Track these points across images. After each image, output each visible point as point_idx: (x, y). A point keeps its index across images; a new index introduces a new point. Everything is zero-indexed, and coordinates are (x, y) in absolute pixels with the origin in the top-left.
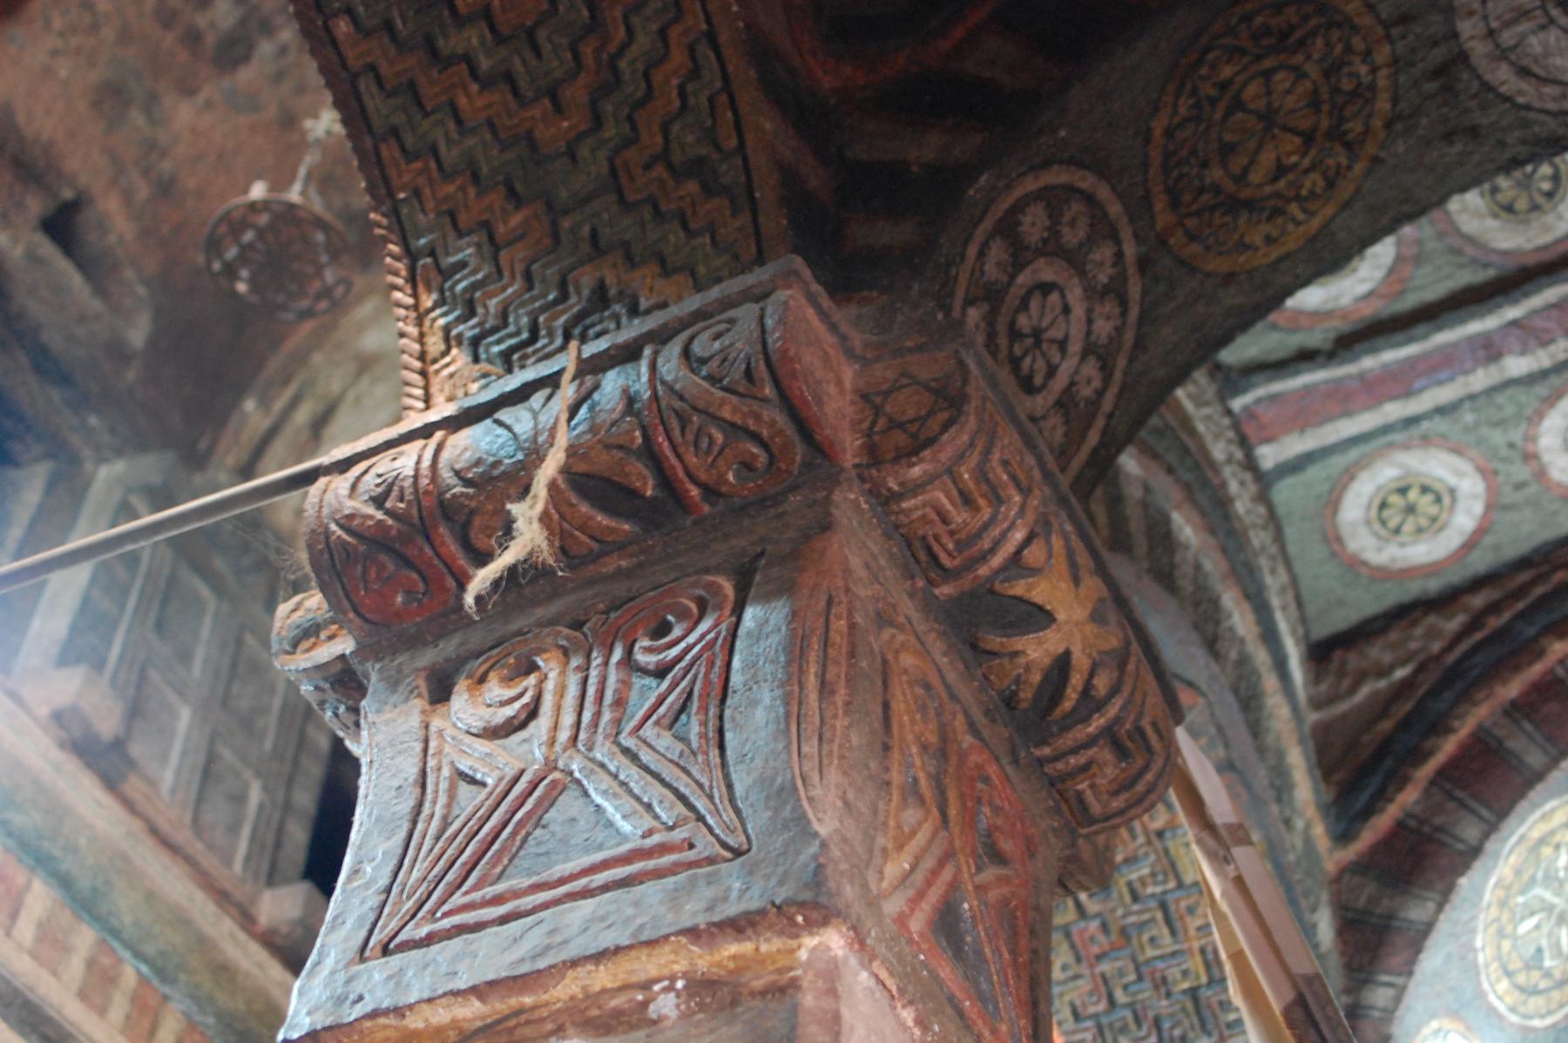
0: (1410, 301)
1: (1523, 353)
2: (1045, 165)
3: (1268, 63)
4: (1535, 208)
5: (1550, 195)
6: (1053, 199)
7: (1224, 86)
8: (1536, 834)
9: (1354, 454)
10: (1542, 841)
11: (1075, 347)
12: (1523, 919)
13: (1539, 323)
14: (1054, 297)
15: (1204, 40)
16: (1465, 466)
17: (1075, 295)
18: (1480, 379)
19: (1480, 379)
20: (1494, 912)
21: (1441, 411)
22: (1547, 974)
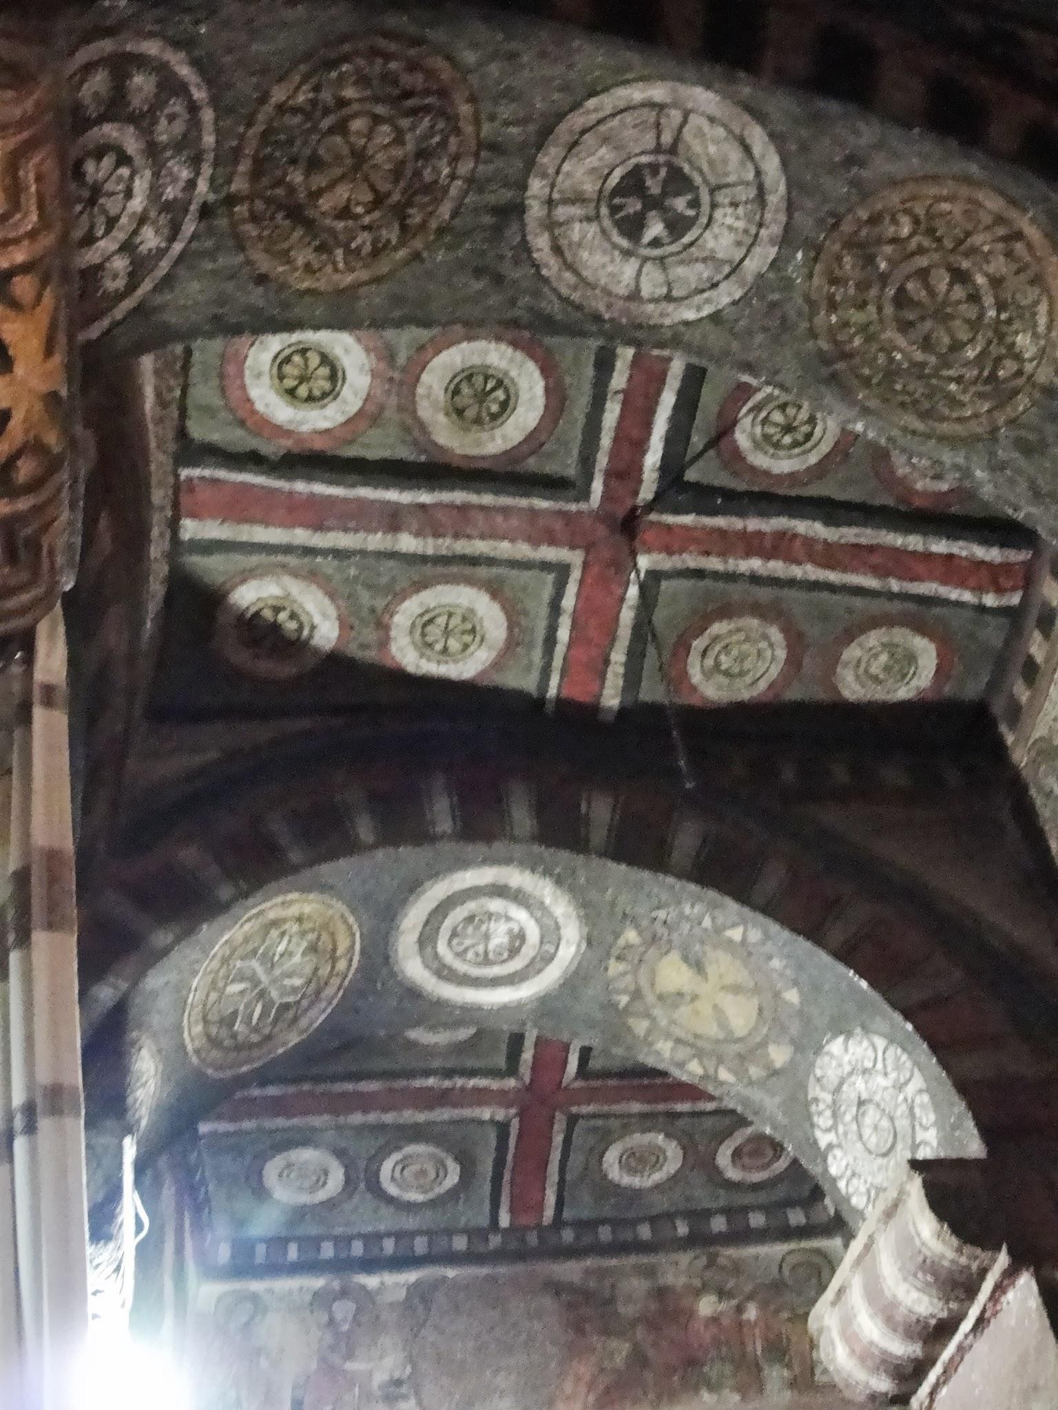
0: (351, 452)
1: (417, 534)
2: (176, 44)
3: (380, 110)
4: (478, 421)
5: (494, 417)
6: (170, 86)
7: (342, 103)
8: (272, 915)
9: (254, 559)
10: (275, 923)
11: (120, 235)
12: (233, 981)
13: (440, 515)
14: (124, 171)
15: (347, 48)
16: (332, 611)
17: (141, 186)
18: (376, 541)
19: (376, 541)
20: (215, 964)
21: (338, 554)
22: (234, 1036)
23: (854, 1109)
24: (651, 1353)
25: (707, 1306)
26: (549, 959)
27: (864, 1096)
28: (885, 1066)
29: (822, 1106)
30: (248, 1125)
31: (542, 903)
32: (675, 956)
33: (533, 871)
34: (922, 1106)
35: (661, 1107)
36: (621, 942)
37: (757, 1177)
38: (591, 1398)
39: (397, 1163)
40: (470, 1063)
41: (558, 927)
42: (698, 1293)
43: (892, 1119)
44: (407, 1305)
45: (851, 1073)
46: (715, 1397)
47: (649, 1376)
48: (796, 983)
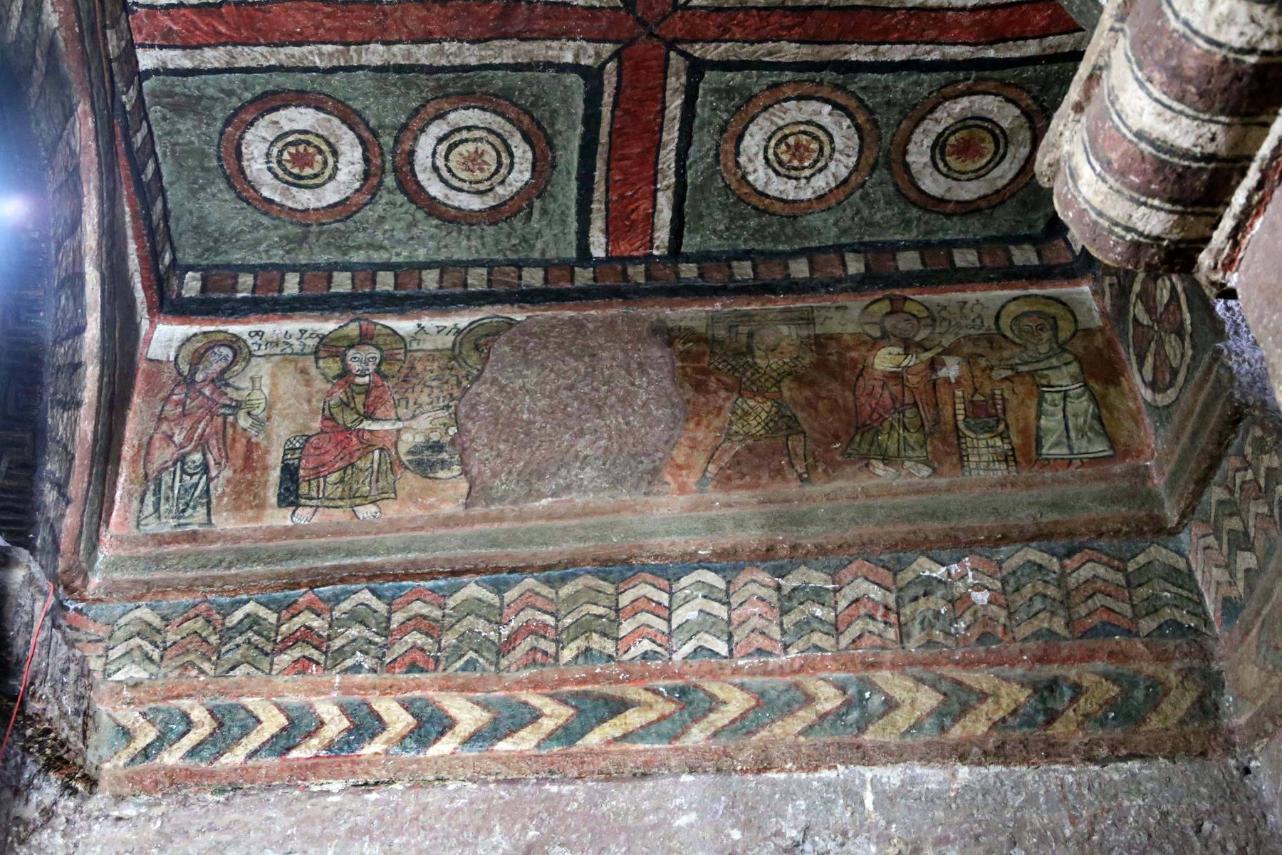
24: (800, 415)
25: (885, 360)
30: (213, 57)
35: (828, 52)
37: (969, 191)
38: (712, 468)
39: (440, 140)
42: (874, 344)
44: (454, 354)
46: (891, 470)
47: (797, 444)
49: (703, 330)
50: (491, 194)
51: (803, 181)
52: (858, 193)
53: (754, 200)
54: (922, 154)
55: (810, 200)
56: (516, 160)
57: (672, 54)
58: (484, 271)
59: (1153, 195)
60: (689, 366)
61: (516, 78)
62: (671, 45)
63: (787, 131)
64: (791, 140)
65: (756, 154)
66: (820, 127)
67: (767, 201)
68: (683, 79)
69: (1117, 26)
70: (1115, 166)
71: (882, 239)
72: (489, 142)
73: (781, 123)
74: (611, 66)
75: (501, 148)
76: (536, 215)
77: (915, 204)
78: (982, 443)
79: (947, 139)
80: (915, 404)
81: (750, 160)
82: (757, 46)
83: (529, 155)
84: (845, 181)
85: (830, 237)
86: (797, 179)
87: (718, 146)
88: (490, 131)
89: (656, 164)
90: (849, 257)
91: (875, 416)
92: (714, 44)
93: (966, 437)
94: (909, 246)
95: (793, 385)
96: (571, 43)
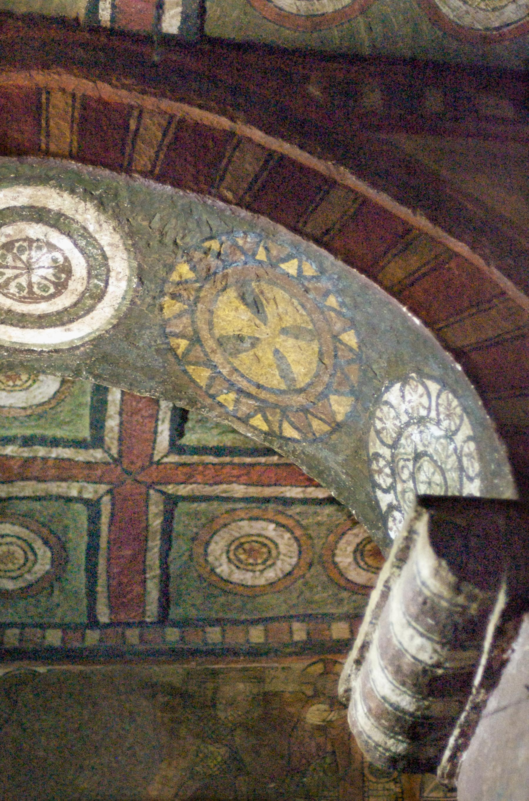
23: (410, 464)
24: (247, 759)
26: (99, 297)
27: (420, 449)
28: (438, 414)
29: (382, 463)
31: (85, 229)
32: (232, 293)
33: (72, 192)
34: (469, 455)
35: (268, 492)
36: (175, 277)
40: (50, 433)
41: (105, 257)
43: (443, 473)
45: (408, 424)
48: (353, 324)
49: (178, 685)
50: (20, 579)
51: (258, 573)
52: (301, 581)
53: (222, 585)
54: (347, 557)
55: (264, 586)
56: (39, 557)
57: (151, 492)
58: (17, 631)
59: (396, 734)
60: (168, 716)
61: (37, 505)
62: (150, 487)
63: (243, 540)
64: (247, 546)
65: (221, 555)
66: (267, 538)
67: (231, 586)
68: (161, 507)
69: (374, 621)
70: (374, 712)
71: (321, 611)
72: (18, 546)
73: (237, 535)
74: (106, 499)
75: (27, 549)
76: (56, 592)
77: (345, 589)
78: (380, 786)
79: (364, 547)
80: (334, 752)
81: (216, 559)
82: (215, 487)
83: (49, 554)
84: (290, 574)
85: (282, 611)
86: (254, 571)
87: (191, 550)
88: (19, 538)
89: (144, 562)
90: (296, 626)
91: (304, 761)
92: (182, 486)
93: (369, 781)
94: (340, 618)
95: (244, 735)
96: (75, 484)
